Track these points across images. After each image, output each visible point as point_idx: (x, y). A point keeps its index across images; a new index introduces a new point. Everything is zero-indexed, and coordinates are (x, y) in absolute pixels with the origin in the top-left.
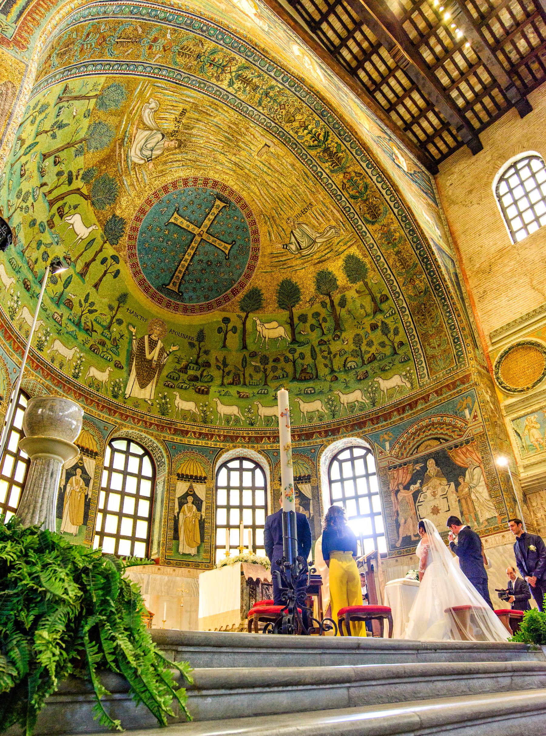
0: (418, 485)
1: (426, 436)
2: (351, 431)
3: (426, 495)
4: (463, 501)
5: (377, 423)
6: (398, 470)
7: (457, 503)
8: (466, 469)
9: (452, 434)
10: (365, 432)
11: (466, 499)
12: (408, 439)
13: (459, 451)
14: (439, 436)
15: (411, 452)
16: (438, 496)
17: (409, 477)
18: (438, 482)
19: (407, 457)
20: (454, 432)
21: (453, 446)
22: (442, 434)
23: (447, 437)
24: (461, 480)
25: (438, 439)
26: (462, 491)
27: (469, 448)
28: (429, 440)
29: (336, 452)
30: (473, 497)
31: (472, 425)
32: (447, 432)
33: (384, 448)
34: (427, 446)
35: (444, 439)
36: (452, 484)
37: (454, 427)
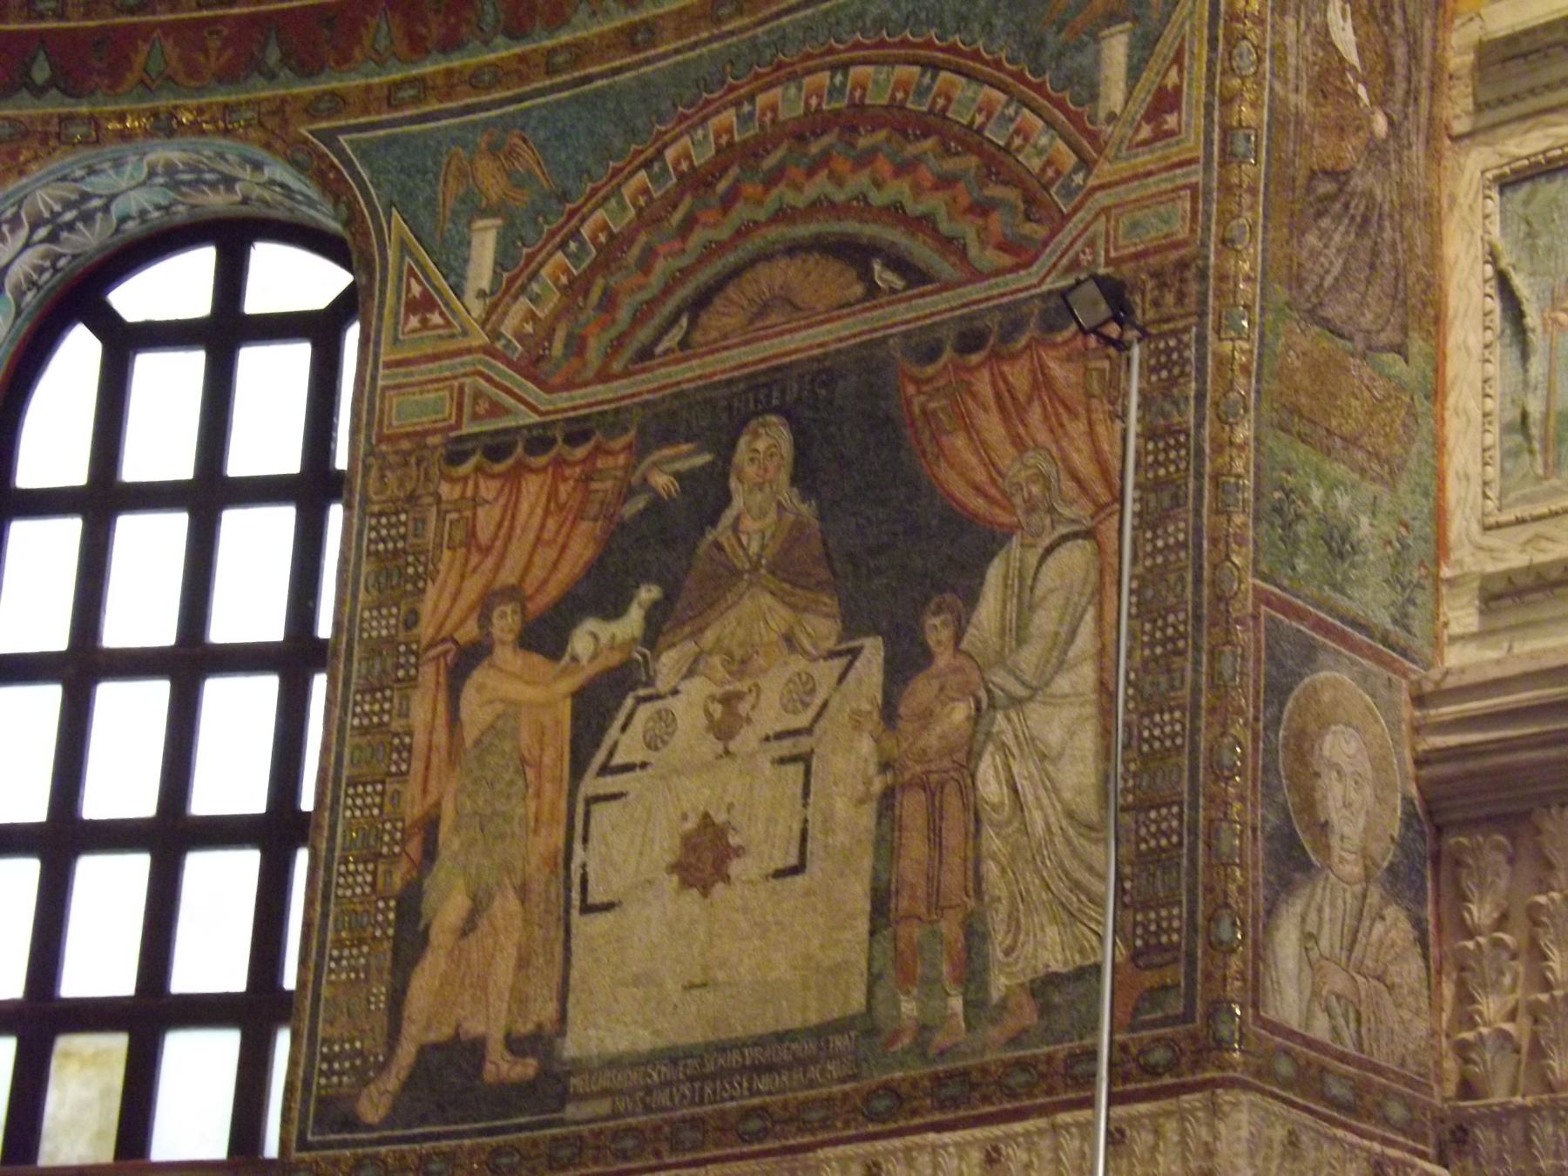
0: (632, 623)
1: (783, 215)
2: (229, 76)
3: (667, 719)
4: (912, 806)
5: (450, 44)
6: (514, 478)
7: (867, 817)
8: (992, 541)
9: (968, 230)
10: (337, 102)
11: (932, 790)
12: (648, 218)
13: (983, 384)
14: (870, 231)
15: (643, 335)
16: (747, 740)
17: (581, 550)
18: (780, 617)
19: (604, 376)
20: (982, 209)
21: (949, 337)
22: (895, 213)
23: (921, 250)
24: (937, 629)
25: (856, 254)
26: (926, 717)
27: (1057, 369)
28: (793, 249)
29: (90, 240)
30: (990, 786)
31: (1123, 167)
32: (934, 203)
33: (455, 271)
34: (764, 309)
35: (899, 264)
36: (873, 650)
37: (997, 163)
